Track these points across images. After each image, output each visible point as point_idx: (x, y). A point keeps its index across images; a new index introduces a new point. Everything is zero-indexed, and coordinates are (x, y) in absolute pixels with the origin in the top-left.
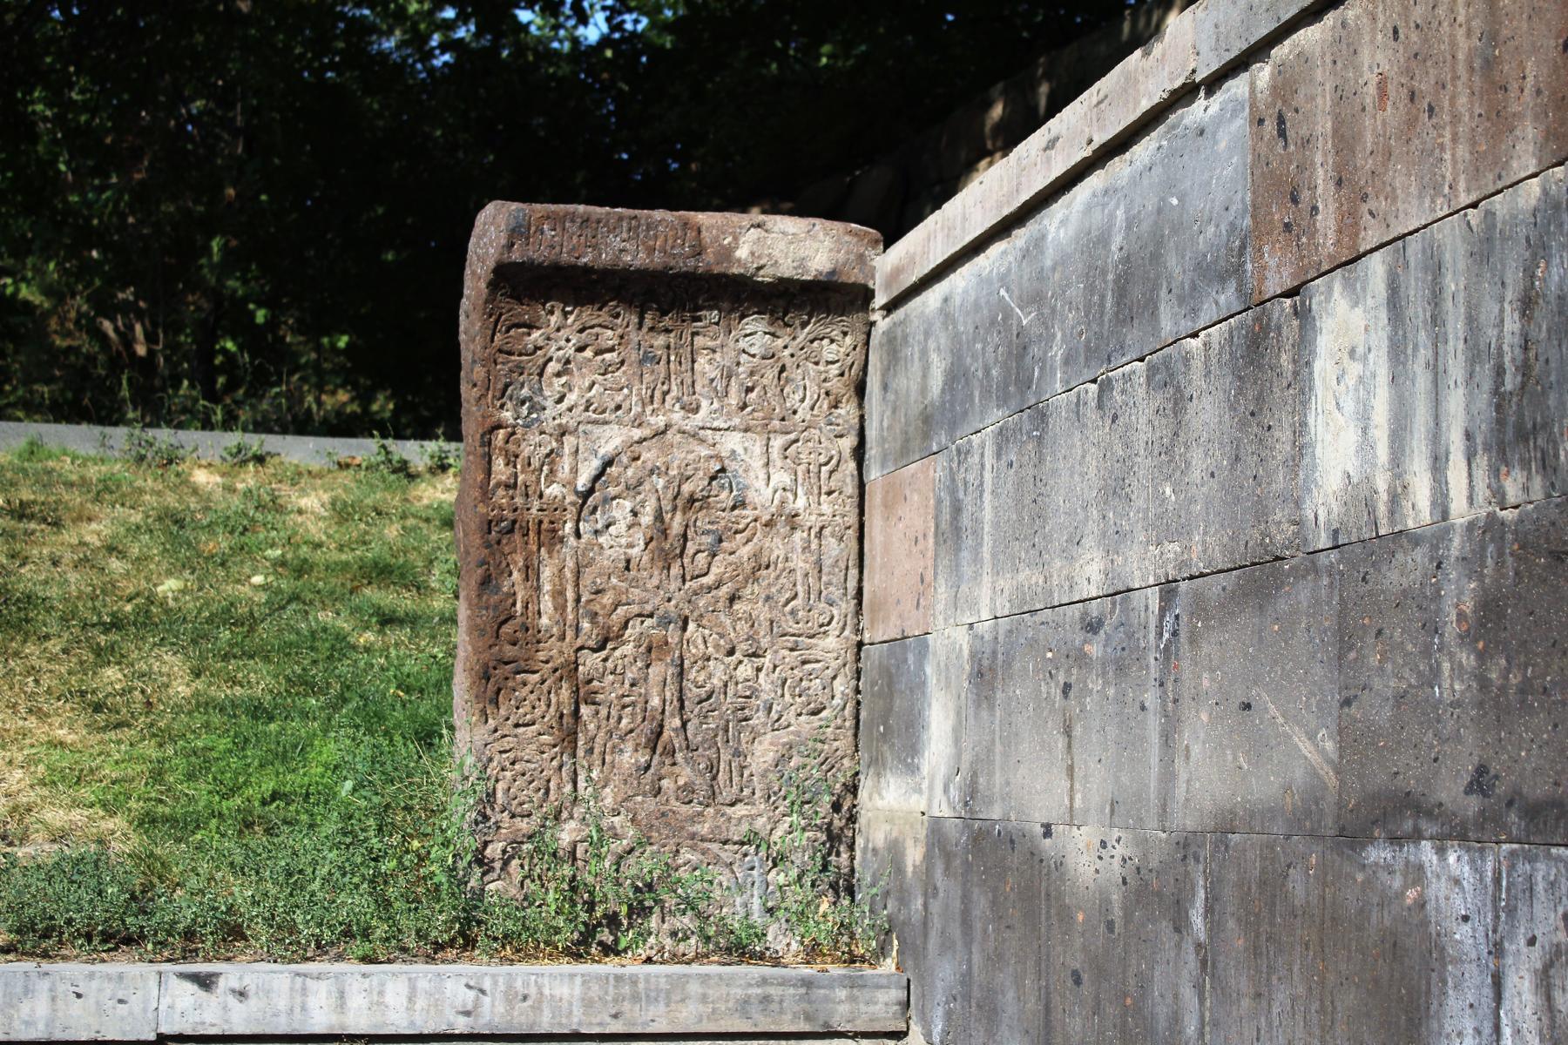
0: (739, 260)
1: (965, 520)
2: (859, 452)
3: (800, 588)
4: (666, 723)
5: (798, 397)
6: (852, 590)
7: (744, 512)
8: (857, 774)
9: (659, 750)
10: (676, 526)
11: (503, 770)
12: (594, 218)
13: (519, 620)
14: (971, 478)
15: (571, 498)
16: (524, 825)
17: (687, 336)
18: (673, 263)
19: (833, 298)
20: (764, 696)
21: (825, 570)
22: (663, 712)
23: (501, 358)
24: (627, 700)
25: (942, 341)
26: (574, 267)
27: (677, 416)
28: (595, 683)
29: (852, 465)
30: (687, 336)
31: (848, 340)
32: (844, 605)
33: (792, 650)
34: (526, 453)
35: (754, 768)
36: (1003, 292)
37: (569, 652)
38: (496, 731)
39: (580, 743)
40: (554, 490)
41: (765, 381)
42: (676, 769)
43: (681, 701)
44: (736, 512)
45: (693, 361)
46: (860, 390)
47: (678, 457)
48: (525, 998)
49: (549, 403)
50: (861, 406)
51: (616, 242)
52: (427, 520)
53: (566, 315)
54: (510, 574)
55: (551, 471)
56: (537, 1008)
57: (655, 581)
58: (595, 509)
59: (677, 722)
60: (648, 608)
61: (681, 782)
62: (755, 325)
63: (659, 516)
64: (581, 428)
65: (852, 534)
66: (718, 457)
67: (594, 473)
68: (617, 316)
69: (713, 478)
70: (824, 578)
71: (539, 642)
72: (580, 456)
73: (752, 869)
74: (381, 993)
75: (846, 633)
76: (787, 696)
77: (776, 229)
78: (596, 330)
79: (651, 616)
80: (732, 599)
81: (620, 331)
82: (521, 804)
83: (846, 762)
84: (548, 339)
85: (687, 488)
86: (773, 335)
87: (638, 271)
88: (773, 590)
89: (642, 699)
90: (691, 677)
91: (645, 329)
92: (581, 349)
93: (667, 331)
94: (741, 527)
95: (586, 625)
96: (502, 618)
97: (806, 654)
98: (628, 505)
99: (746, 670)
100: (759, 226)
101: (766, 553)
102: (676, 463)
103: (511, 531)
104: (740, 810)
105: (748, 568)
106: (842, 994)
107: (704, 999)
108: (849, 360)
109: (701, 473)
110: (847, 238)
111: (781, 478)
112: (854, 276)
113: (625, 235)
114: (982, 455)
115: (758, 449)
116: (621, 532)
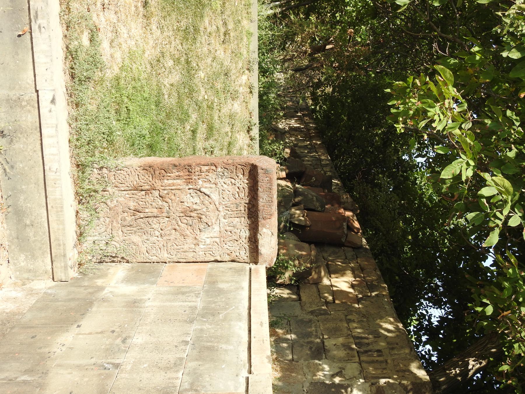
1: (180, 296)
2: (217, 261)
3: (179, 247)
5: (230, 245)
6: (180, 260)
9: (135, 212)
10: (193, 214)
13: (166, 175)
14: (189, 298)
15: (199, 187)
16: (112, 178)
17: (244, 215)
19: (255, 254)
20: (151, 238)
24: (147, 203)
25: (232, 287)
27: (222, 214)
29: (213, 259)
30: (244, 215)
36: (234, 307)
37: (157, 188)
40: (200, 182)
43: (148, 217)
46: (233, 261)
47: (211, 214)
49: (223, 180)
50: (229, 261)
51: (265, 197)
52: (231, 138)
53: (247, 184)
60: (171, 208)
61: (126, 218)
62: (248, 234)
63: (195, 210)
65: (195, 260)
66: (212, 225)
74: (53, 147)
76: (151, 244)
80: (175, 229)
81: (244, 198)
83: (135, 260)
85: (203, 217)
92: (238, 188)
95: (166, 192)
97: (162, 249)
98: (198, 202)
99: (157, 233)
101: (188, 238)
103: (189, 172)
104: (120, 233)
105: (183, 233)
106: (63, 265)
107: (59, 229)
108: (240, 258)
111: (208, 241)
112: (260, 259)
114: (193, 302)
115: (215, 235)
116: (191, 200)
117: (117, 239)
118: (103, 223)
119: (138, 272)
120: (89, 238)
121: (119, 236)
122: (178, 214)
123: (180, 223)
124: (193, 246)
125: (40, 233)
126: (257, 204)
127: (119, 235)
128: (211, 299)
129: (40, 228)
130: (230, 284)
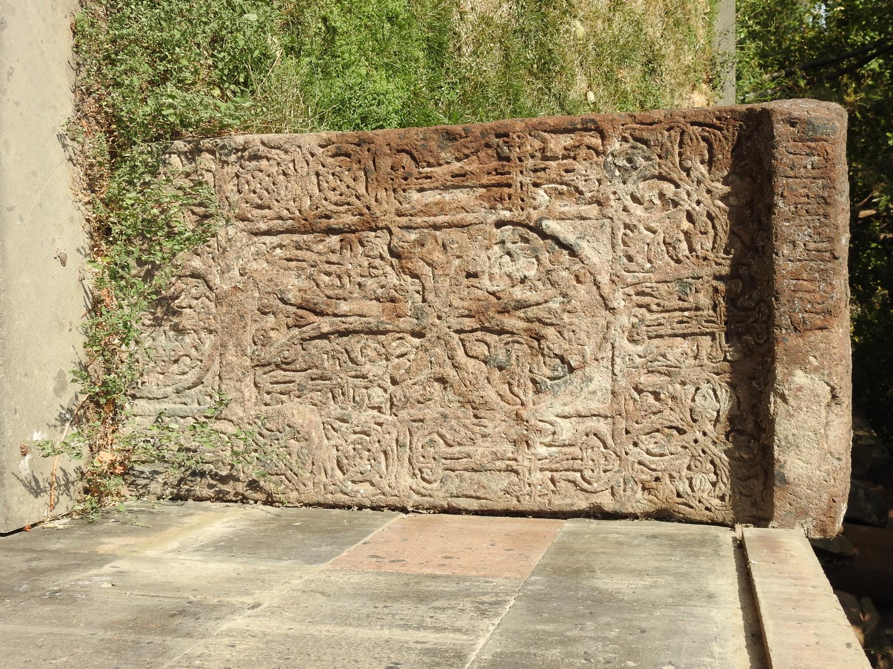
0: (791, 374)
1: (405, 609)
2: (598, 513)
3: (456, 449)
4: (326, 319)
5: (651, 446)
7: (531, 393)
8: (283, 503)
9: (301, 312)
10: (511, 322)
11: (278, 164)
12: (829, 210)
13: (415, 171)
15: (535, 215)
18: (783, 300)
20: (355, 415)
21: (475, 475)
22: (336, 315)
23: (676, 135)
24: (346, 280)
25: (660, 591)
26: (772, 193)
27: (624, 320)
28: (360, 249)
29: (582, 503)
31: (717, 502)
32: (441, 494)
33: (397, 441)
34: (577, 166)
35: (289, 404)
38: (313, 155)
39: (305, 237)
40: (541, 196)
41: (667, 412)
42: (284, 329)
44: (530, 385)
45: (684, 336)
47: (582, 322)
49: (630, 187)
50: (648, 516)
54: (458, 160)
55: (561, 193)
57: (457, 303)
58: (526, 240)
59: (326, 329)
60: (430, 297)
61: (272, 334)
63: (521, 305)
64: (607, 221)
65: (512, 503)
66: (584, 363)
67: (561, 237)
68: (727, 252)
69: (562, 359)
70: (467, 474)
71: (395, 191)
72: (578, 222)
73: (199, 404)
75: (416, 497)
77: (832, 417)
78: (711, 232)
79: (424, 301)
80: (442, 380)
81: (711, 256)
82: (247, 182)
83: (294, 495)
84: (699, 182)
85: (550, 332)
86: (717, 420)
87: (772, 263)
88: (454, 422)
89: (347, 295)
90: (370, 343)
91: (715, 283)
92: (690, 217)
93: (715, 307)
94: (516, 389)
95: (413, 236)
96: (415, 153)
97: (393, 455)
98: (532, 273)
99: (378, 396)
100: (834, 397)
101: (489, 414)
102: (576, 321)
103: (501, 158)
104: (250, 392)
105: (473, 396)
108: (695, 503)
109: (567, 346)
110: (825, 497)
111: (566, 430)
112: (781, 505)
113: (812, 246)
115: (595, 406)
116: (505, 268)
117: (236, 411)
118: (193, 352)
119: (289, 526)
120: (142, 405)
121: (242, 403)
122: (455, 323)
123: (460, 352)
124: (509, 447)
126: (770, 270)
127: (246, 400)
128: (549, 628)
130: (648, 581)
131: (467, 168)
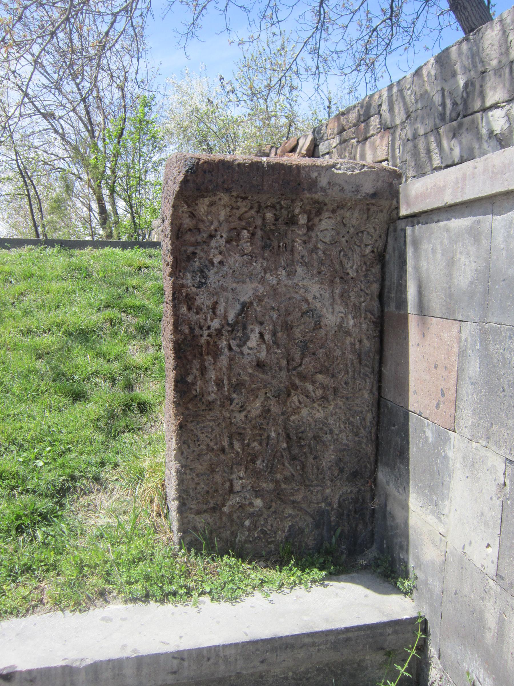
48: (209, 659)
56: (216, 664)
125: (319, 678)
129: (308, 679)
131: (198, 367)
